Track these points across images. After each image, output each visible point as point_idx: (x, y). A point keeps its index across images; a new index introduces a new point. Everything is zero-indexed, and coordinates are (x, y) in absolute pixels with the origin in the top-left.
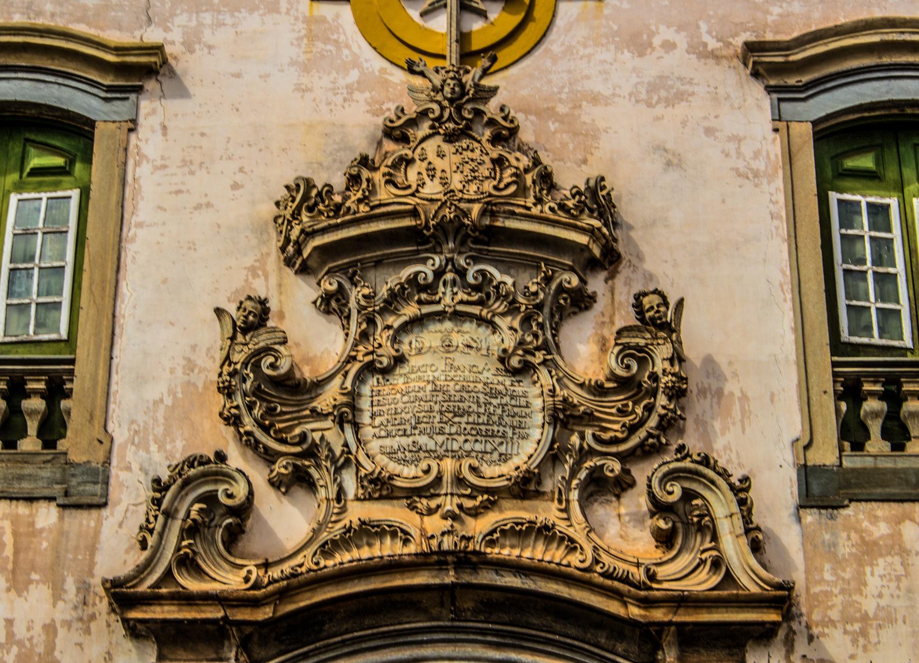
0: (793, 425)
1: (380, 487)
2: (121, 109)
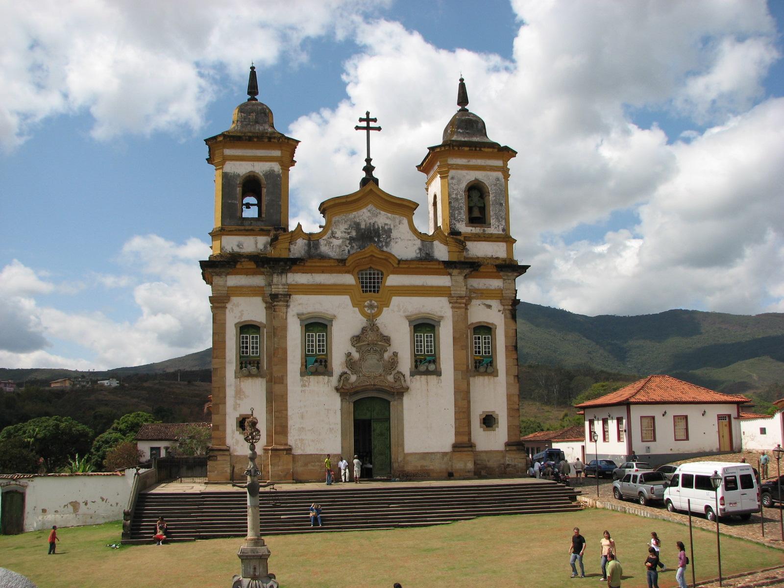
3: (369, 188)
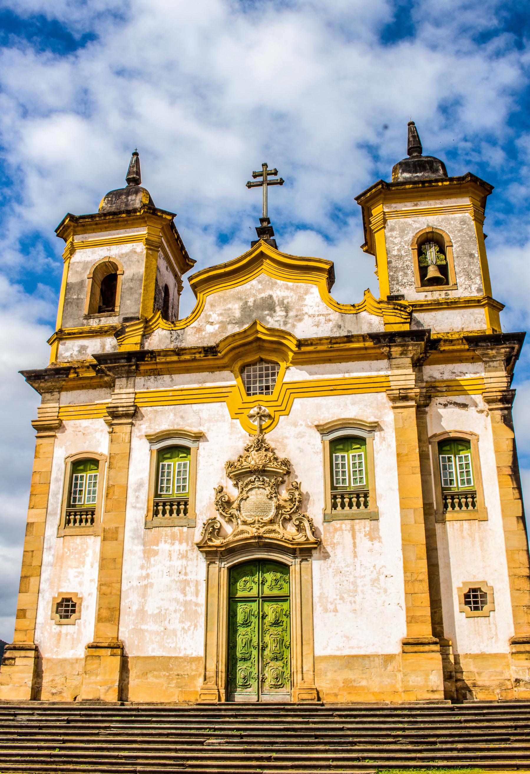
0: (323, 506)
1: (245, 523)
2: (196, 445)
3: (258, 252)
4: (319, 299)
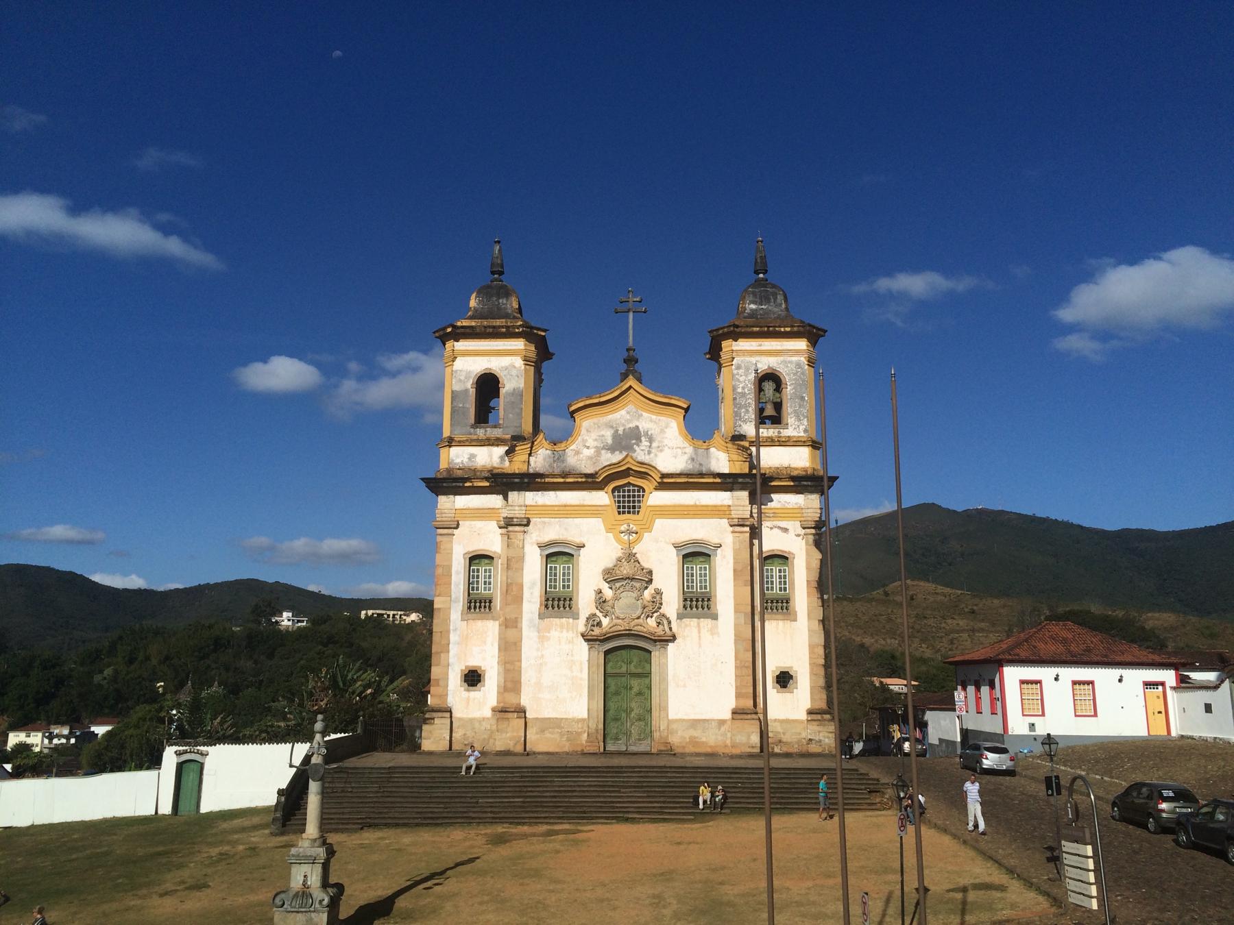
0: (676, 606)
1: (618, 618)
4: (677, 433)
